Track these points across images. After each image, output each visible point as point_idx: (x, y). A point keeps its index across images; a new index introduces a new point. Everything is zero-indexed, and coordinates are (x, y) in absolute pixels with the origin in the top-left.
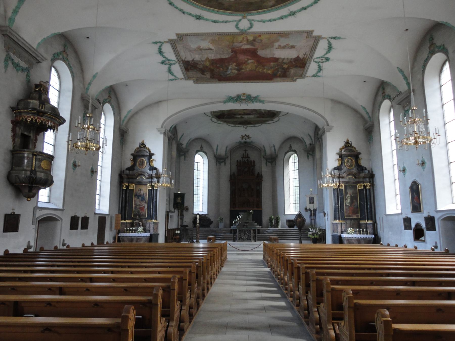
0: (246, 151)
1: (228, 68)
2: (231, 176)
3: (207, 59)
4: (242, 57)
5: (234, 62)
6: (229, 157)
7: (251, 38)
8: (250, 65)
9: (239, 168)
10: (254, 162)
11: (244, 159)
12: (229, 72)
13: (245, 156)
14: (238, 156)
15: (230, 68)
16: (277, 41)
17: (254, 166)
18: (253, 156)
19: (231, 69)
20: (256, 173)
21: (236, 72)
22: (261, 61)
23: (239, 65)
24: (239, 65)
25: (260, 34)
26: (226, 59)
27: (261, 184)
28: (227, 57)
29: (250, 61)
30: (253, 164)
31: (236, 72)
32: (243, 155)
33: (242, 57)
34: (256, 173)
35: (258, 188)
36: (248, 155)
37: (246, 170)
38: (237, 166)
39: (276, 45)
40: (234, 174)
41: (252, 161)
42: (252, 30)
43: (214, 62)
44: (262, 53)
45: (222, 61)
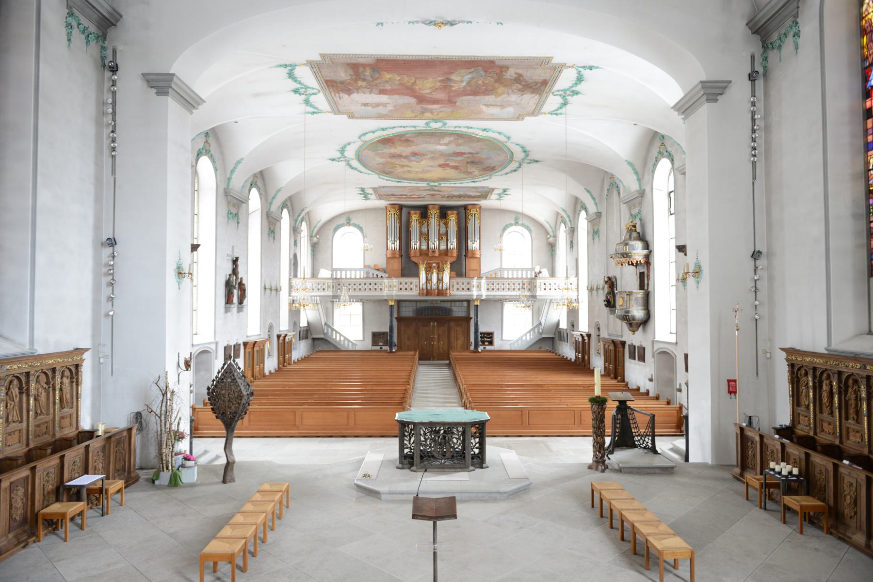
1: (468, 83)
3: (497, 95)
4: (441, 95)
5: (455, 91)
7: (427, 115)
8: (427, 85)
12: (467, 78)
15: (464, 84)
16: (390, 111)
19: (462, 81)
21: (453, 77)
22: (410, 91)
23: (446, 84)
24: (446, 84)
25: (416, 118)
26: (467, 95)
28: (465, 98)
29: (428, 91)
31: (453, 77)
33: (441, 95)
39: (390, 108)
42: (425, 121)
43: (487, 91)
44: (413, 100)
45: (475, 93)
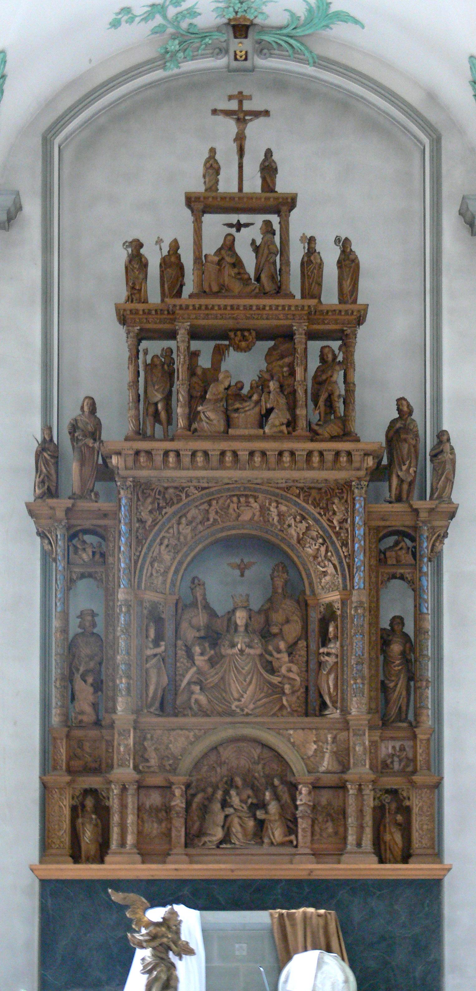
0: (242, 117)
2: (47, 453)
6: (32, 209)
9: (154, 347)
10: (348, 263)
11: (215, 226)
13: (227, 184)
14: (145, 198)
17: (344, 324)
18: (341, 198)
20: (373, 422)
27: (436, 557)
30: (330, 296)
32: (212, 168)
34: (373, 422)
35: (396, 603)
36: (269, 169)
37: (244, 366)
38: (139, 321)
40: (86, 429)
41: (330, 256)
